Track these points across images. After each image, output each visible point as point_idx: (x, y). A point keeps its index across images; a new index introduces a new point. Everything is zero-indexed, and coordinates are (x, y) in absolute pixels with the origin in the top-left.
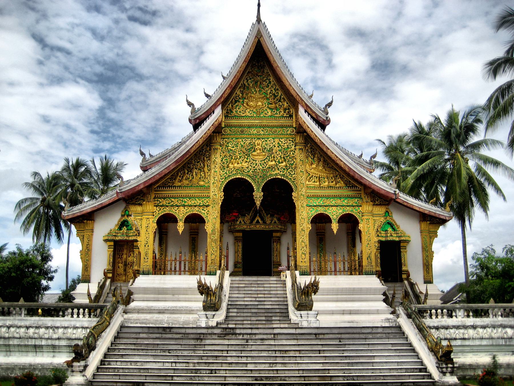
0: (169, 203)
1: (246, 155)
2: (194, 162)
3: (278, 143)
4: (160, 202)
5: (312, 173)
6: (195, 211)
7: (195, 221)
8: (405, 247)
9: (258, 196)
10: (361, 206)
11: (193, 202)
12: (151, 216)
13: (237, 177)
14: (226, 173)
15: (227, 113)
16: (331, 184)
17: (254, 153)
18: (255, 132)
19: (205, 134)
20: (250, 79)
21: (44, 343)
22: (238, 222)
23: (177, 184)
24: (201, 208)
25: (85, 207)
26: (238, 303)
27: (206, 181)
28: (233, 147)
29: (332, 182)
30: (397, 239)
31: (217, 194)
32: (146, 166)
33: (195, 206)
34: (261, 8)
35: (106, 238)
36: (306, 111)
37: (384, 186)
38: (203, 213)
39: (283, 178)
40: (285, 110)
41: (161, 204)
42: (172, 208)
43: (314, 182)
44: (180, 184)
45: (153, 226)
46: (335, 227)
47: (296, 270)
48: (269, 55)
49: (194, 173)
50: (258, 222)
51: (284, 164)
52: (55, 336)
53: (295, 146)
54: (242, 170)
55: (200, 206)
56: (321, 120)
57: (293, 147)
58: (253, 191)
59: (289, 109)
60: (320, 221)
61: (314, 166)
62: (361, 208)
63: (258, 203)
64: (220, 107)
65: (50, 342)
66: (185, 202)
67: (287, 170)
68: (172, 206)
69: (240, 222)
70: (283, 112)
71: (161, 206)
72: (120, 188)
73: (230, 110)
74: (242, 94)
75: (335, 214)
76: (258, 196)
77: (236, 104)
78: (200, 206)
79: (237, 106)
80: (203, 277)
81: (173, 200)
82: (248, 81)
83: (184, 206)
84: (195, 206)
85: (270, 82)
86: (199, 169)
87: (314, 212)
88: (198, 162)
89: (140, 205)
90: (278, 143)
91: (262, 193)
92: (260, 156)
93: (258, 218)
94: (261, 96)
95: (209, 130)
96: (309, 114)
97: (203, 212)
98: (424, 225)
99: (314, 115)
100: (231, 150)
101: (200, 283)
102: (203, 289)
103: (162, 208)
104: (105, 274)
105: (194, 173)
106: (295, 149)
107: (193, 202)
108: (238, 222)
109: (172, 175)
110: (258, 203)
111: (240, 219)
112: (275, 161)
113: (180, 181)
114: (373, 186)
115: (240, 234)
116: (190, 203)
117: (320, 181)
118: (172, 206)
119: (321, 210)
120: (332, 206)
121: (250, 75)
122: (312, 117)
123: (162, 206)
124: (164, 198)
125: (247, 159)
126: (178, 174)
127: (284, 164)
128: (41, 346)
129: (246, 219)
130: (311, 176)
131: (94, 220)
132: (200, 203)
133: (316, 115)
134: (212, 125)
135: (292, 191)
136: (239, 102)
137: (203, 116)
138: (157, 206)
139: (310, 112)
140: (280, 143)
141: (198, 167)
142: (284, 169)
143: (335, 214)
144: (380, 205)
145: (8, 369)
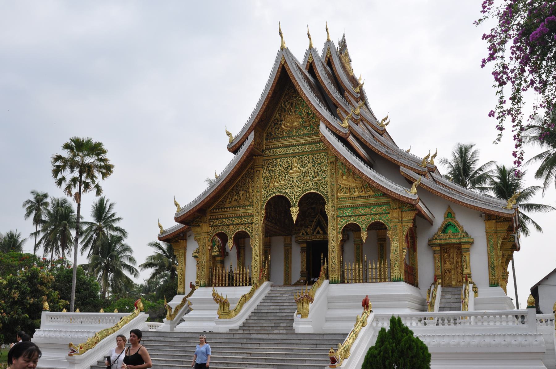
2: (241, 184)
5: (343, 184)
6: (241, 229)
8: (468, 250)
9: (295, 212)
11: (240, 221)
12: (206, 236)
14: (267, 192)
15: (268, 136)
16: (361, 194)
17: (291, 171)
20: (287, 101)
22: (301, 234)
23: (227, 205)
24: (247, 226)
26: (263, 311)
27: (251, 200)
28: (273, 167)
29: (362, 191)
30: (458, 241)
33: (242, 224)
34: (283, 35)
35: (194, 255)
36: (327, 127)
38: (248, 230)
41: (215, 224)
43: (345, 193)
44: (230, 205)
46: (364, 236)
47: (327, 278)
49: (241, 195)
50: (318, 232)
55: (245, 224)
60: (350, 230)
61: (344, 177)
63: (295, 218)
64: (253, 133)
66: (233, 221)
68: (223, 225)
69: (303, 234)
71: (215, 226)
73: (270, 133)
74: (280, 116)
75: (363, 223)
76: (295, 212)
77: (276, 126)
78: (245, 224)
79: (276, 128)
80: (215, 288)
81: (224, 220)
82: (285, 103)
83: (233, 224)
84: (242, 224)
87: (343, 223)
88: (244, 184)
89: (199, 226)
90: (313, 159)
91: (298, 209)
93: (318, 229)
94: (296, 116)
96: (329, 129)
98: (492, 223)
99: (334, 130)
100: (271, 170)
101: (214, 294)
102: (218, 299)
104: (192, 286)
105: (241, 195)
108: (301, 234)
109: (224, 198)
110: (295, 218)
111: (303, 231)
113: (230, 203)
115: (305, 245)
116: (237, 222)
117: (350, 192)
118: (223, 225)
119: (351, 220)
120: (361, 215)
121: (287, 97)
122: (332, 132)
123: (215, 226)
124: (217, 219)
125: (285, 177)
126: (228, 197)
127: (318, 178)
129: (309, 230)
130: (342, 188)
131: (186, 240)
135: (324, 203)
136: (277, 124)
138: (211, 227)
141: (245, 188)
143: (363, 223)
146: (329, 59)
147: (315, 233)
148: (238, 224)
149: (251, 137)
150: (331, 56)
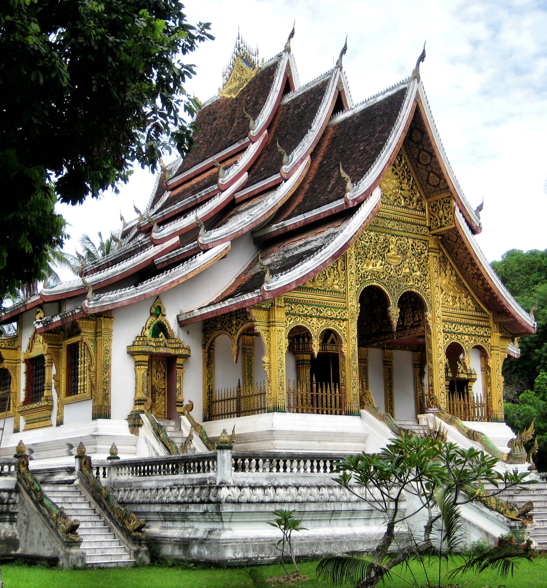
0: (303, 311)
1: (381, 255)
3: (412, 245)
4: (292, 309)
9: (394, 312)
10: (490, 337)
13: (373, 284)
19: (363, 223)
25: (121, 296)
32: (207, 244)
33: (331, 319)
37: (526, 317)
39: (417, 291)
40: (418, 201)
42: (305, 318)
44: (311, 286)
45: (285, 343)
51: (418, 273)
53: (428, 252)
54: (373, 273)
55: (336, 319)
56: (474, 226)
57: (426, 254)
59: (421, 201)
62: (489, 340)
65: (350, 506)
66: (321, 312)
67: (422, 282)
68: (306, 316)
70: (415, 204)
71: (293, 315)
72: (269, 285)
76: (394, 312)
78: (336, 319)
83: (318, 317)
84: (331, 319)
85: (401, 160)
86: (332, 268)
91: (399, 310)
92: (394, 258)
95: (368, 218)
97: (340, 328)
103: (293, 318)
106: (428, 255)
107: (329, 313)
110: (395, 322)
112: (410, 269)
114: (517, 316)
122: (466, 221)
125: (382, 260)
128: (339, 512)
132: (337, 316)
134: (371, 212)
137: (361, 197)
139: (465, 215)
140: (414, 244)
142: (418, 281)
145: (312, 544)
146: (288, 79)
147: (329, 341)
148: (326, 318)
149: (377, 194)
150: (291, 76)
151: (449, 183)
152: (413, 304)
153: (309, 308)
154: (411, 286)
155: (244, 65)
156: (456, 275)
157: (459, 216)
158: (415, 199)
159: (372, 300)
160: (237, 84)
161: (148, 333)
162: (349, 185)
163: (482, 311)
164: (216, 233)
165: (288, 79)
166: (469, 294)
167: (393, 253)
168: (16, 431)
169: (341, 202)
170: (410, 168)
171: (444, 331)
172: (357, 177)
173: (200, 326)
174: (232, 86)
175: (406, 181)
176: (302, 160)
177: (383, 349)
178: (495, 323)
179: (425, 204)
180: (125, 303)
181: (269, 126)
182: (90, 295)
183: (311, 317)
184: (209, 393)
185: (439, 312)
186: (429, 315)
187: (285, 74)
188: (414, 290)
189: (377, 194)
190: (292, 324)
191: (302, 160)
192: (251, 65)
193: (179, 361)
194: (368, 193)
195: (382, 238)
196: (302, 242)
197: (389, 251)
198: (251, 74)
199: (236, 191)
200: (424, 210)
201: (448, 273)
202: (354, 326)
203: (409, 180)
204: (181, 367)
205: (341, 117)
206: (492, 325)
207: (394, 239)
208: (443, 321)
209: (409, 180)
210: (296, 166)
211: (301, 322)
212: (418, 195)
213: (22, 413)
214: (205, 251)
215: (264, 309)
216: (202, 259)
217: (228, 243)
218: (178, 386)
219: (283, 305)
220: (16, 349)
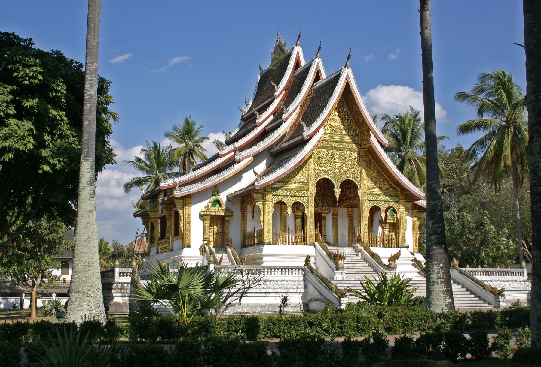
6: (299, 200)
7: (297, 206)
9: (337, 191)
18: (335, 146)
21: (271, 291)
25: (193, 188)
31: (313, 190)
38: (304, 201)
40: (354, 130)
44: (287, 180)
48: (354, 94)
52: (277, 287)
55: (302, 197)
58: (334, 187)
60: (374, 210)
63: (337, 196)
65: (275, 290)
68: (284, 196)
76: (337, 191)
78: (302, 197)
85: (344, 109)
87: (371, 205)
110: (337, 196)
114: (411, 191)
122: (378, 141)
133: (381, 140)
143: (383, 206)
144: (409, 202)
145: (253, 307)
146: (298, 61)
151: (367, 121)
152: (349, 186)
153: (286, 192)
154: (349, 176)
155: (280, 52)
156: (377, 169)
157: (373, 139)
158: (351, 130)
159: (324, 187)
160: (277, 61)
161: (210, 205)
162: (305, 128)
163: (394, 188)
164: (244, 153)
165: (298, 61)
166: (386, 179)
167: (337, 160)
168: (157, 253)
169: (300, 137)
170: (349, 113)
171: (368, 200)
172: (309, 124)
173: (239, 199)
174: (275, 63)
175: (346, 120)
176: (294, 110)
177: (348, 208)
178: (401, 194)
179: (358, 131)
180: (196, 191)
181: (286, 89)
182: (177, 188)
183: (287, 196)
184: (244, 233)
185: (365, 190)
186: (359, 192)
187: (296, 59)
188: (350, 179)
189: (321, 131)
190: (275, 200)
191: (294, 110)
192: (283, 51)
193: (227, 218)
194: (317, 131)
195: (330, 152)
196: (287, 156)
197: (335, 159)
198: (282, 57)
199: (266, 126)
200: (357, 136)
201: (372, 168)
202: (312, 200)
203: (348, 120)
204: (228, 221)
205: (318, 84)
206: (400, 195)
207: (338, 153)
208: (368, 194)
209: (348, 120)
210: (291, 114)
211: (281, 199)
212: (354, 127)
213: (159, 244)
214: (238, 163)
215: (261, 193)
216: (237, 167)
217: (252, 158)
218: (226, 231)
219: (270, 190)
220: (156, 212)
